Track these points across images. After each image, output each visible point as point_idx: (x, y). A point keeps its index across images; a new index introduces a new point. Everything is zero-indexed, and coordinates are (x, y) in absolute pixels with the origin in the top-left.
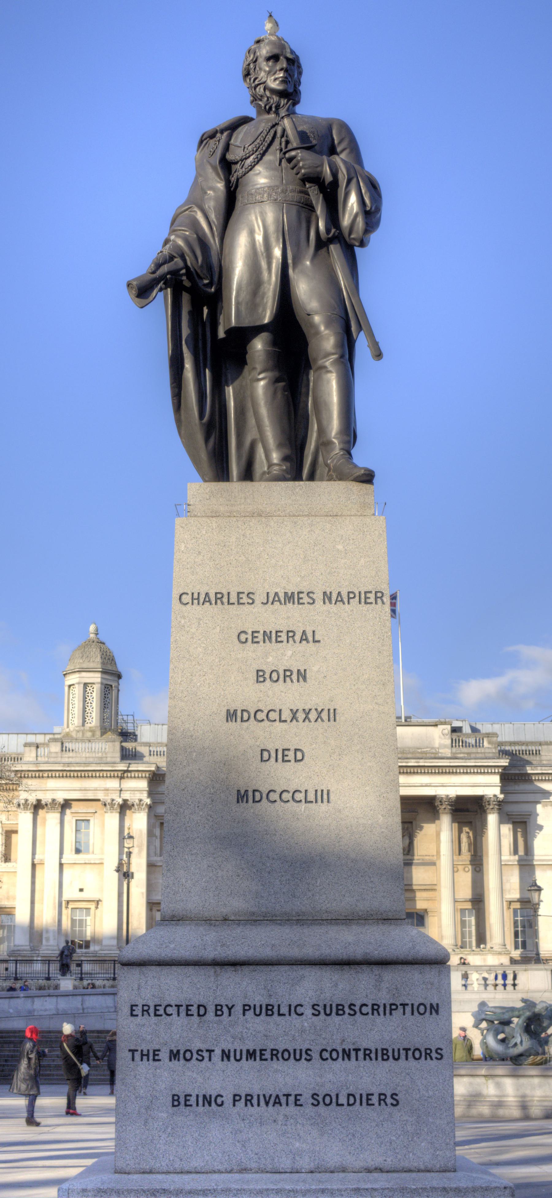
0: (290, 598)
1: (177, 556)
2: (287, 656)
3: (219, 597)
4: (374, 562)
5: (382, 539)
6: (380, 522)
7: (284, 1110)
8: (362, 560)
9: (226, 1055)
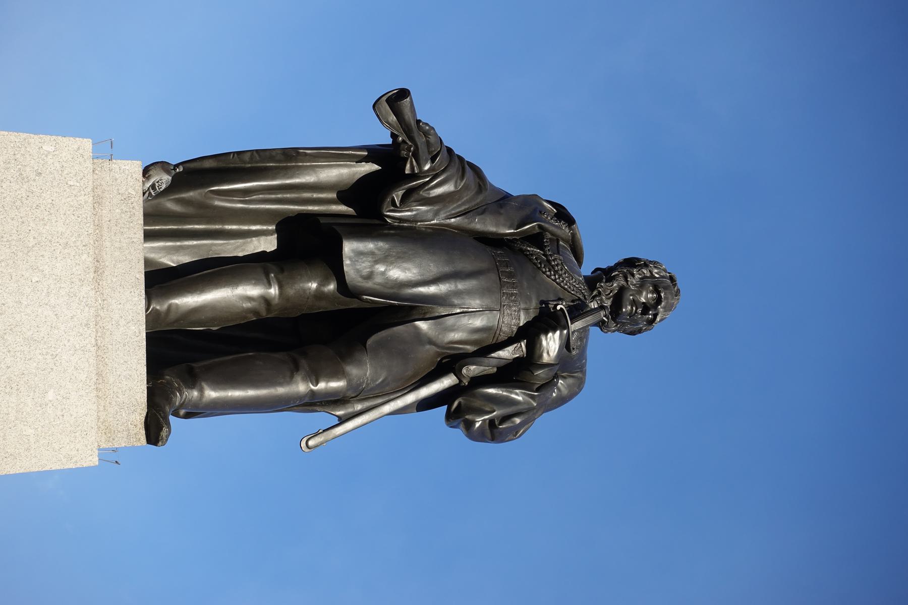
1: (34, 139)
4: (28, 449)
5: (64, 460)
6: (93, 460)
8: (30, 431)
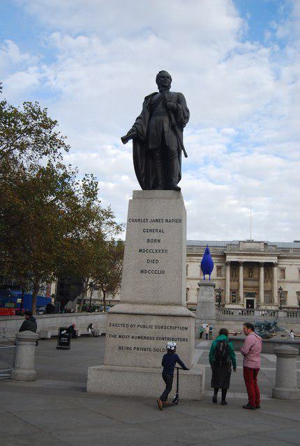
0: (157, 220)
2: (155, 236)
3: (139, 220)
7: (146, 352)
9: (133, 337)
